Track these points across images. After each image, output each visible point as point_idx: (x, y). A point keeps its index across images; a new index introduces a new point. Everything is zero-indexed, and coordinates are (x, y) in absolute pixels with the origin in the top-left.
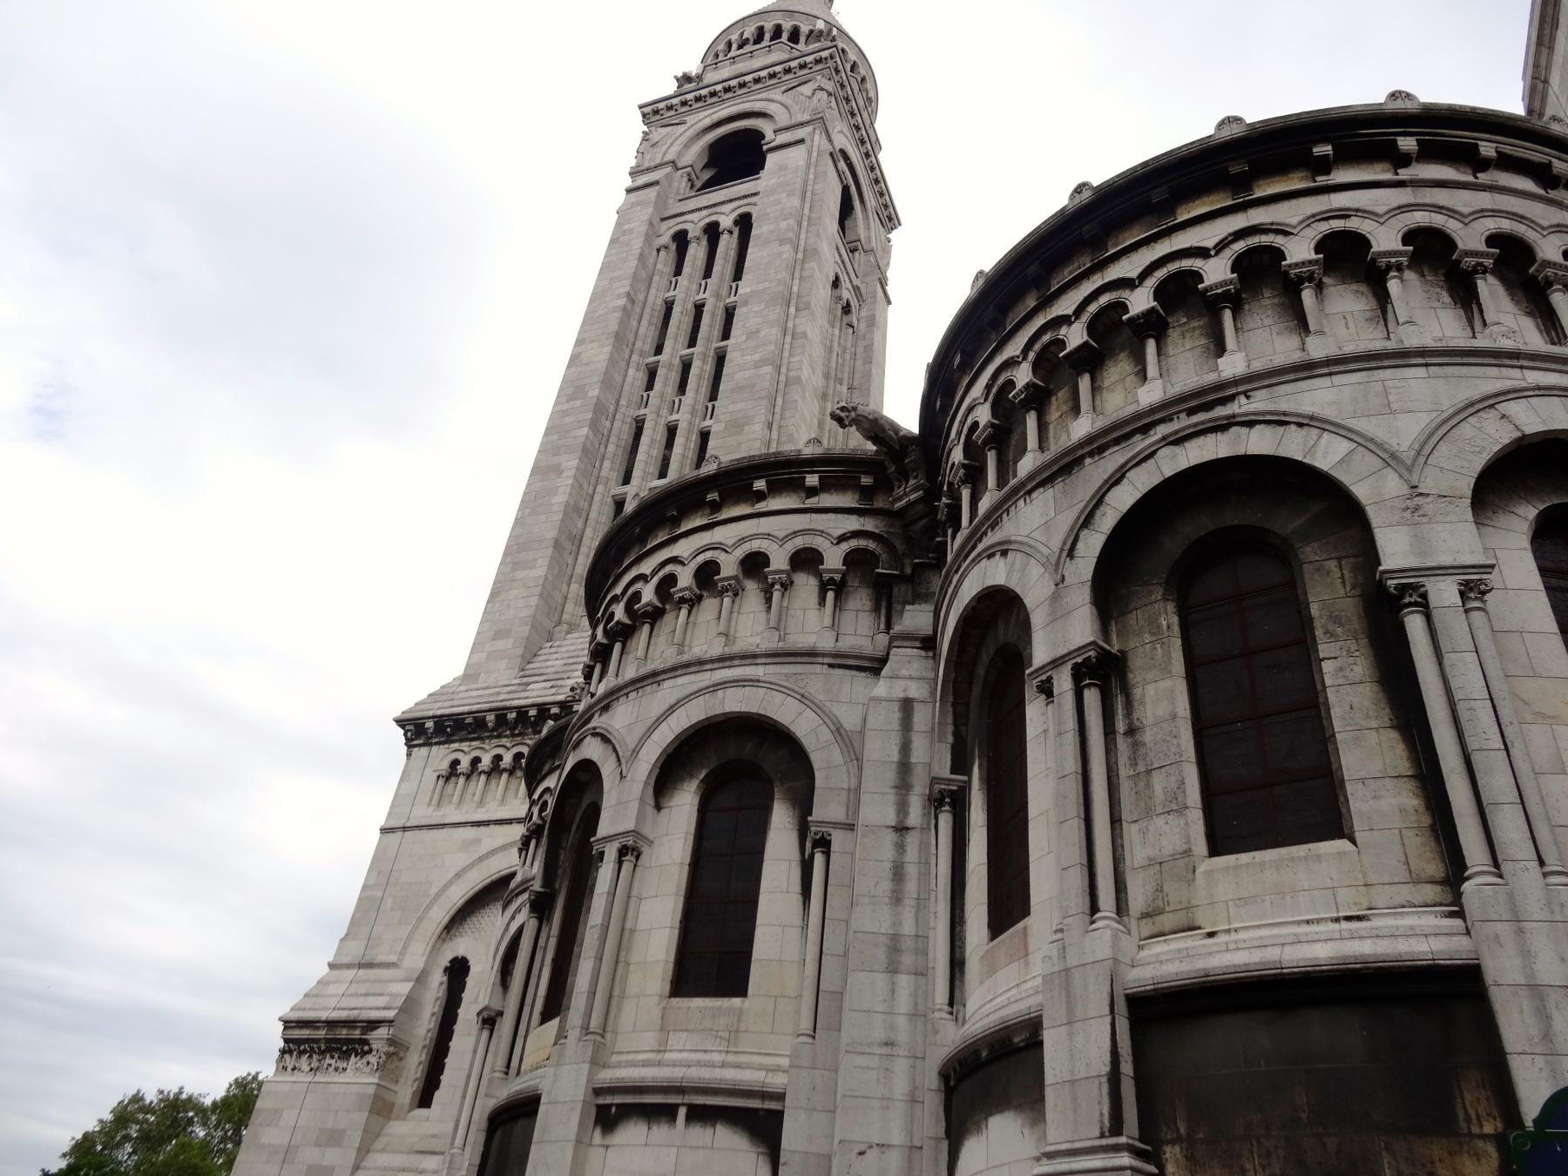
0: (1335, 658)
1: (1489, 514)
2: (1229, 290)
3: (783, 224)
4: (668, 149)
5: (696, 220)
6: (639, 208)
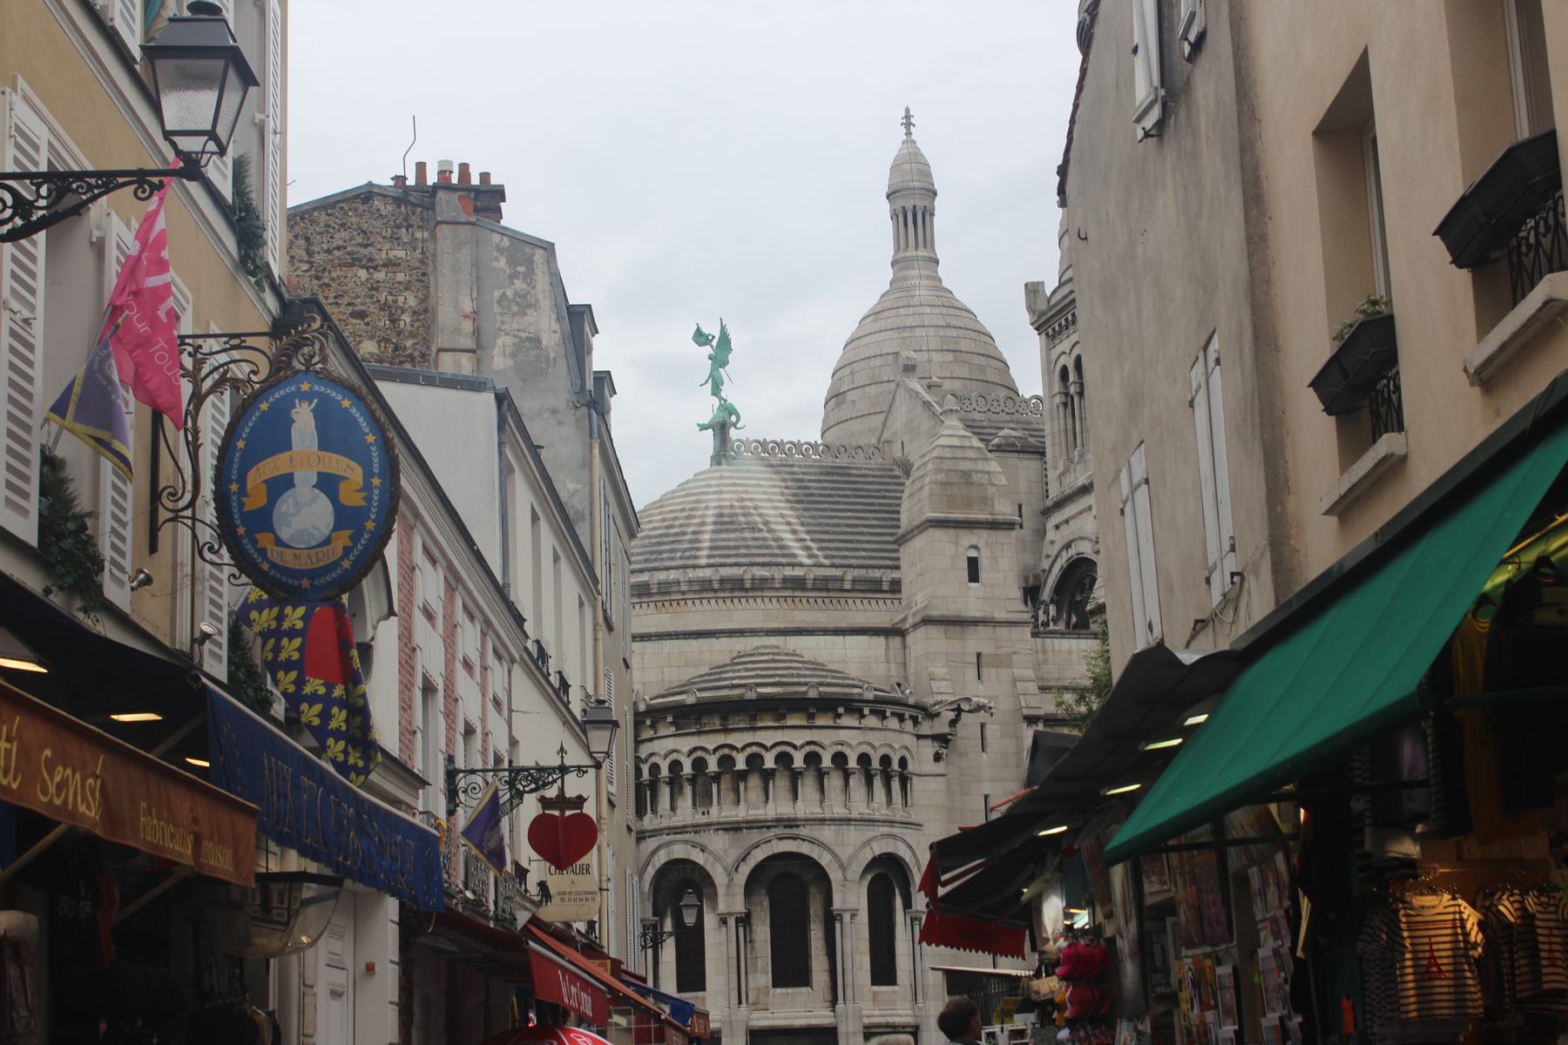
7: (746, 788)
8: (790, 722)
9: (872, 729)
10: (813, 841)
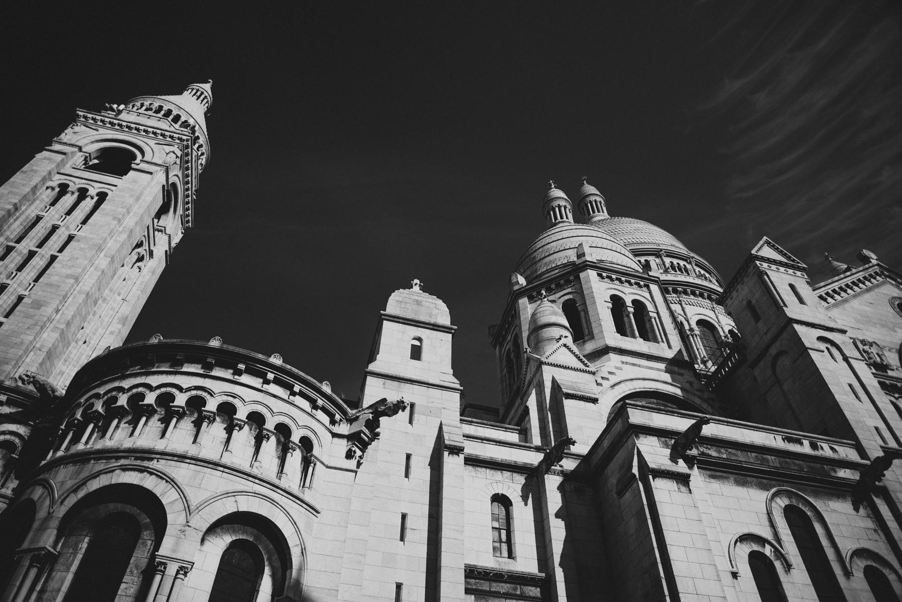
0: (127, 583)
1: (214, 537)
2: (180, 410)
3: (120, 210)
4: (82, 139)
5: (77, 183)
6: (47, 162)
7: (117, 427)
8: (185, 369)
9: (275, 396)
10: (161, 476)
